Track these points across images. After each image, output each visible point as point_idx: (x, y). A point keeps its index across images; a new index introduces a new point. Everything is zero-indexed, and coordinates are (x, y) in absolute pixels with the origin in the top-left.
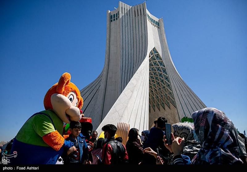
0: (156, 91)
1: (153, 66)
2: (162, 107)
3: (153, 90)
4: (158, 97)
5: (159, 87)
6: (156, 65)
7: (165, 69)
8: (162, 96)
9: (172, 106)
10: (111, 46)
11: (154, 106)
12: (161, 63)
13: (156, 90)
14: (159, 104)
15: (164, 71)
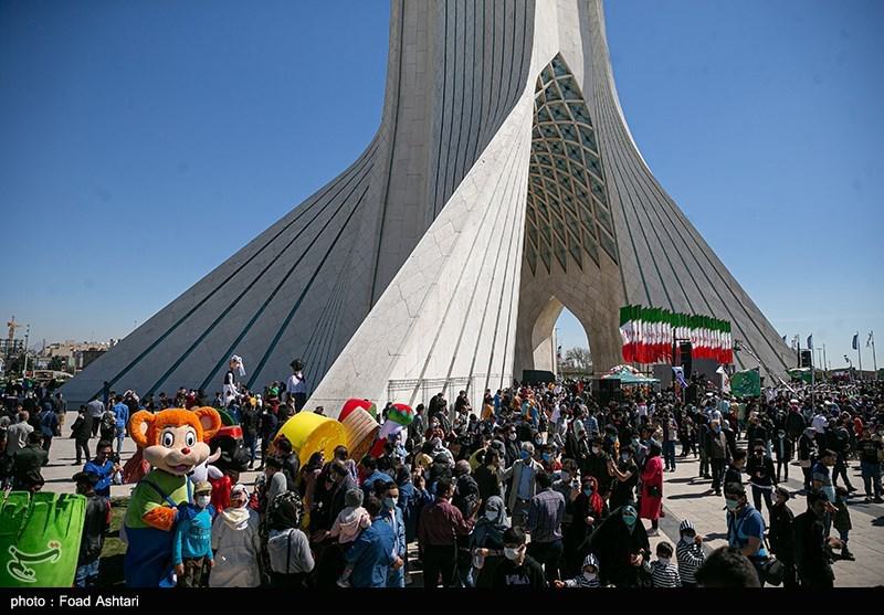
0: (555, 207)
1: (550, 120)
2: (573, 260)
3: (547, 204)
4: (561, 226)
5: (569, 193)
6: (559, 117)
7: (593, 132)
8: (574, 223)
9: (605, 259)
10: (407, 48)
11: (549, 254)
12: (580, 112)
13: (556, 203)
14: (566, 248)
15: (589, 139)
